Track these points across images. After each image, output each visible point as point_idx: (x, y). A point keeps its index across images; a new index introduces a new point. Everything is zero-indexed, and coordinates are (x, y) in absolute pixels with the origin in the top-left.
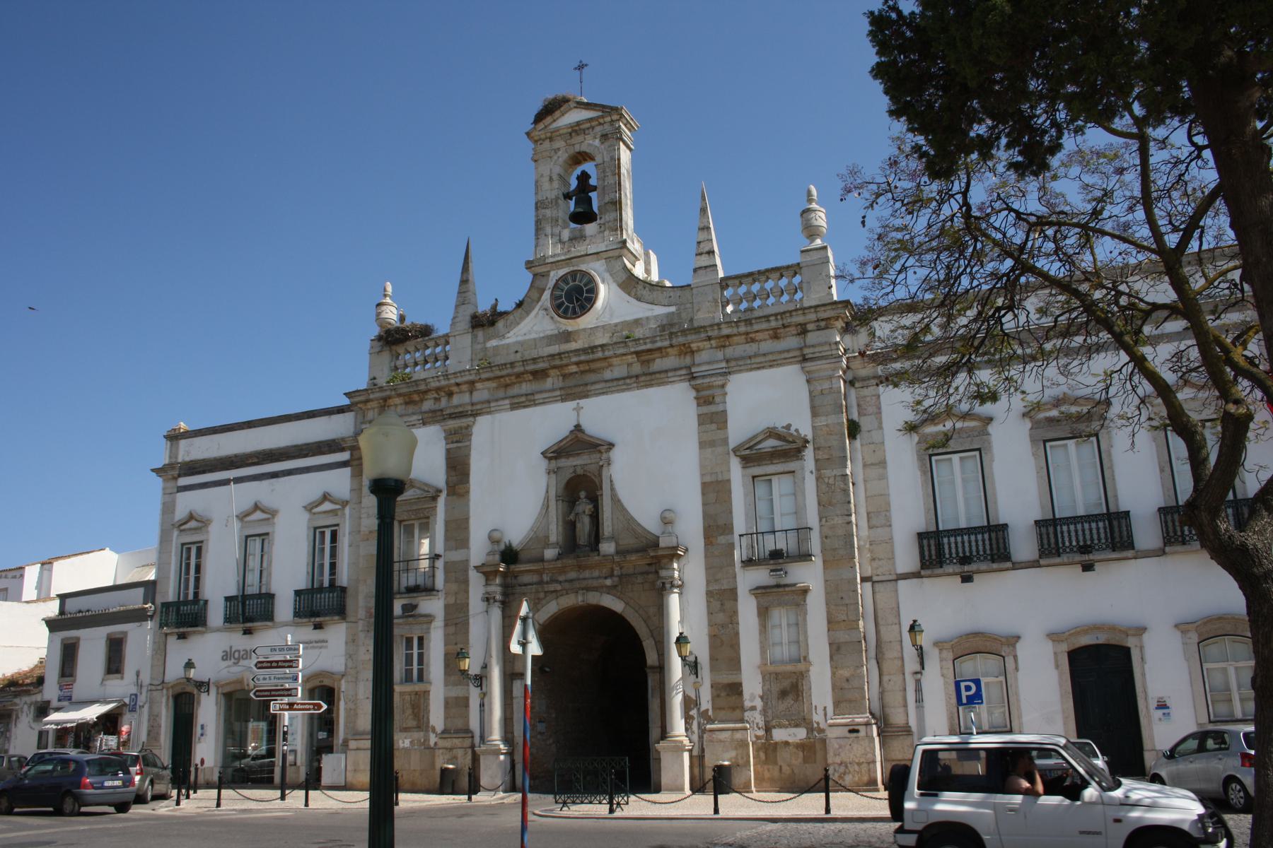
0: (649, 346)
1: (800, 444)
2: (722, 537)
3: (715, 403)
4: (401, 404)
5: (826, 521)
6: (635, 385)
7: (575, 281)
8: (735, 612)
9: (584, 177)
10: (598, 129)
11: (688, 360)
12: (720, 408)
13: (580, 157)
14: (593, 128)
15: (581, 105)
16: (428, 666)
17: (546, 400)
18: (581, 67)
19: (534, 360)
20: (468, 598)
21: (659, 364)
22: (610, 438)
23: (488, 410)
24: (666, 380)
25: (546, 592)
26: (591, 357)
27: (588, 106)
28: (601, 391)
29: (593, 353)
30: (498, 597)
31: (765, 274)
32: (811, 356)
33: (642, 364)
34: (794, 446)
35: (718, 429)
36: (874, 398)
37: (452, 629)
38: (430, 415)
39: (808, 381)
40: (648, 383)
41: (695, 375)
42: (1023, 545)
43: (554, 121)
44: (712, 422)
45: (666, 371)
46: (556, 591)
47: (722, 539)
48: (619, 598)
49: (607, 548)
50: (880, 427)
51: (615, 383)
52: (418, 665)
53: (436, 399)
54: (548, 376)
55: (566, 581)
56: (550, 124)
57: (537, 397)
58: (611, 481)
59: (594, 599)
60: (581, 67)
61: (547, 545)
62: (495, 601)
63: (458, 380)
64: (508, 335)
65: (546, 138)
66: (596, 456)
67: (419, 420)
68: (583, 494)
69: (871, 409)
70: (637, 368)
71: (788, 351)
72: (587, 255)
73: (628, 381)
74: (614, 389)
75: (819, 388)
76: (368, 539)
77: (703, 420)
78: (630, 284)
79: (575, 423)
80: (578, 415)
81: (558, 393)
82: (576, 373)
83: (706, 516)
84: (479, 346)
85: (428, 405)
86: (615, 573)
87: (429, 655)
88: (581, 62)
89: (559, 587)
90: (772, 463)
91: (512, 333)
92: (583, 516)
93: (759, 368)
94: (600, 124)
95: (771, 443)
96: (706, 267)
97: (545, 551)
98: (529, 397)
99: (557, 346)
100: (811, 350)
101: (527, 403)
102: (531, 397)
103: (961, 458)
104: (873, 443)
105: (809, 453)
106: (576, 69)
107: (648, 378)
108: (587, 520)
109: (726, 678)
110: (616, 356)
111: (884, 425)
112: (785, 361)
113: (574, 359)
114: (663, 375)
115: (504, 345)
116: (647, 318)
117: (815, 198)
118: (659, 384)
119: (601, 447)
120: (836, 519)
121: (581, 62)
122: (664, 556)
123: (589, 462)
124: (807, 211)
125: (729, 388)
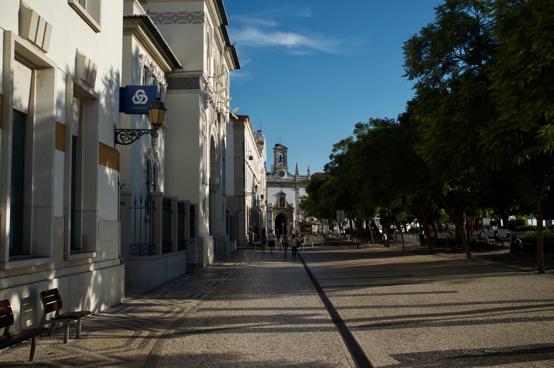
9: (280, 156)
21: (292, 185)
31: (303, 176)
49: (286, 207)
59: (283, 212)
70: (289, 185)
77: (296, 193)
78: (289, 174)
95: (304, 197)
119: (285, 194)
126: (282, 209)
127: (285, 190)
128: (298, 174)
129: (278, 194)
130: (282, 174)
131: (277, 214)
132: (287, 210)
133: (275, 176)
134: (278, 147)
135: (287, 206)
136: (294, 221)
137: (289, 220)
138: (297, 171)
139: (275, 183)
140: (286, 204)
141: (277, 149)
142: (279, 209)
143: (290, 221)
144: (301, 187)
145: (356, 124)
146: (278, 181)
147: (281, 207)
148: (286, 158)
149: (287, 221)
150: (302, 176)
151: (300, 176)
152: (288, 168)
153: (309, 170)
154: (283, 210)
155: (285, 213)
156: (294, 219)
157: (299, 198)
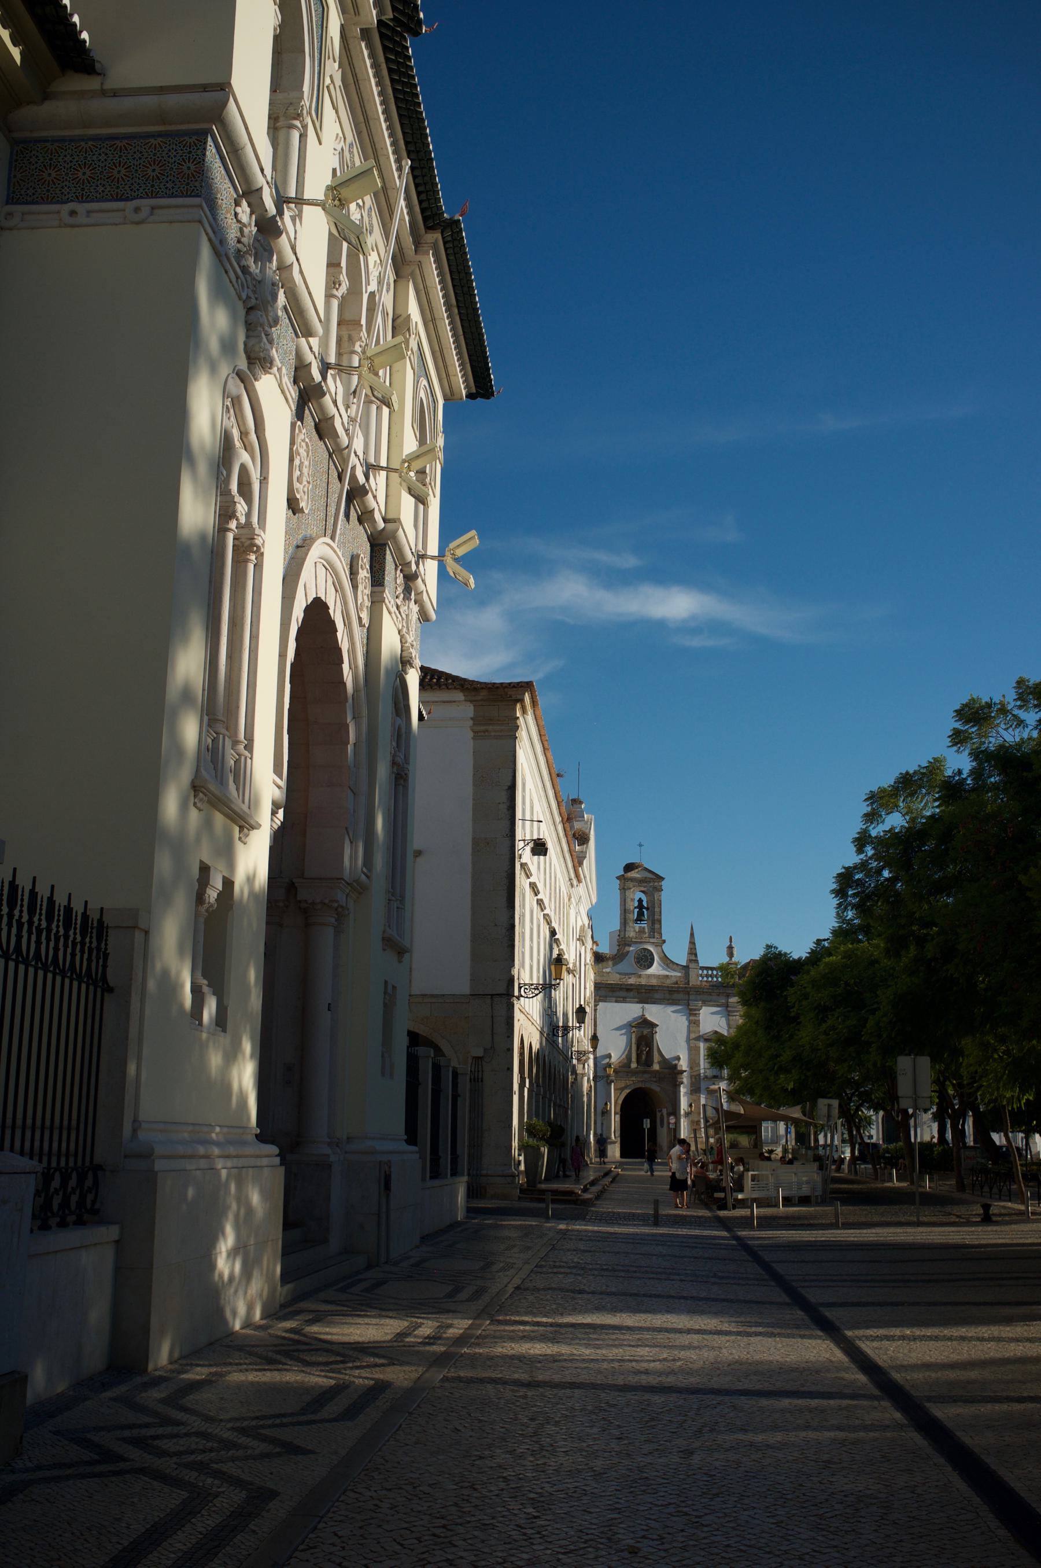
9: (640, 901)
12: (698, 1019)
14: (650, 882)
21: (676, 996)
49: (656, 1067)
59: (648, 1085)
68: (643, 1043)
70: (668, 996)
77: (690, 1022)
78: (667, 961)
109: (696, 1119)
126: (645, 1072)
127: (654, 1012)
128: (696, 961)
129: (630, 1025)
130: (645, 959)
131: (628, 1091)
132: (658, 1076)
133: (622, 967)
134: (633, 874)
135: (659, 1063)
136: (682, 1112)
137: (665, 1111)
138: (693, 952)
139: (621, 989)
140: (656, 1058)
141: (632, 879)
142: (634, 1073)
143: (669, 1114)
144: (705, 1003)
145: (958, 707)
146: (632, 981)
147: (641, 1068)
148: (657, 909)
149: (659, 1115)
150: (707, 968)
151: (703, 968)
152: (664, 941)
153: (730, 948)
154: (646, 1076)
155: (655, 1087)
156: (682, 1107)
157: (698, 1038)
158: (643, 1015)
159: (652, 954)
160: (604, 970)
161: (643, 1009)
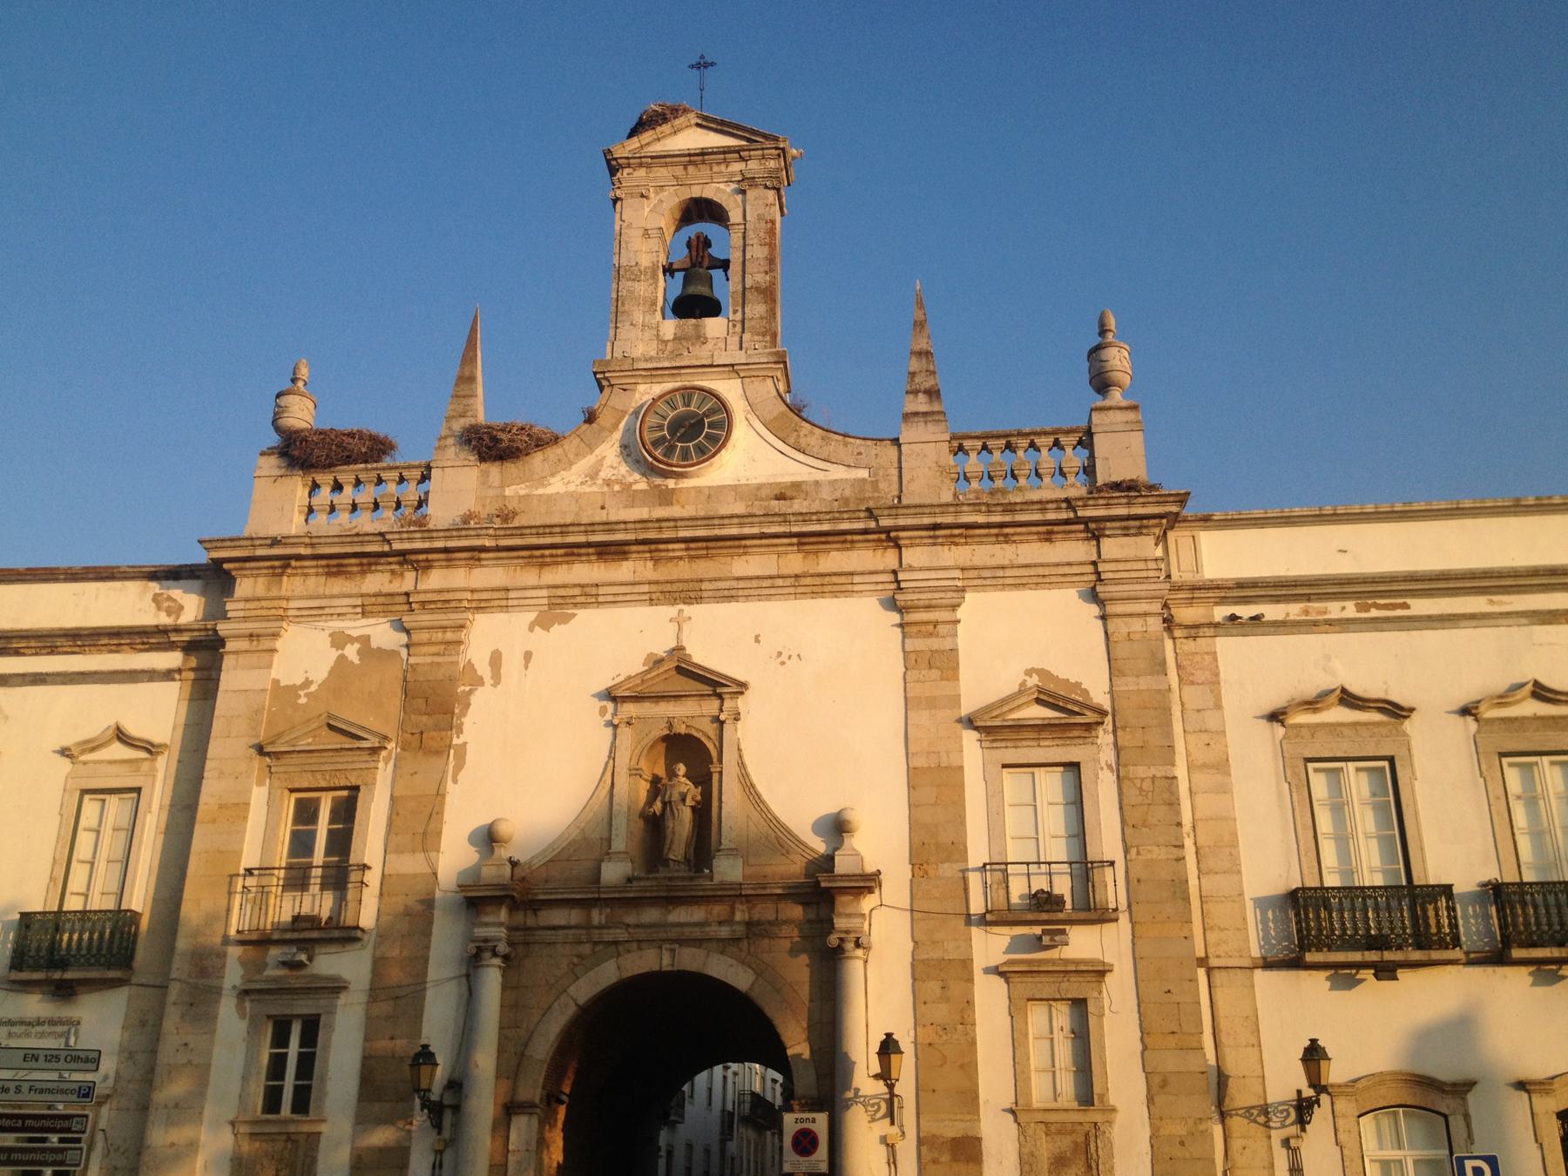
0: (826, 527)
1: (1091, 717)
2: (946, 865)
3: (937, 636)
4: (317, 575)
5: (1138, 853)
6: (792, 590)
7: (689, 406)
8: (970, 1003)
10: (737, 167)
11: (889, 559)
12: (946, 644)
13: (700, 210)
14: (727, 162)
15: (709, 123)
16: (323, 1079)
17: (620, 598)
18: (702, 65)
19: (609, 526)
20: (428, 947)
21: (834, 560)
22: (741, 677)
23: (504, 603)
24: (850, 587)
25: (596, 943)
26: (717, 532)
27: (722, 127)
28: (726, 593)
29: (722, 526)
30: (502, 948)
32: (1111, 575)
33: (804, 557)
34: (1079, 720)
35: (942, 679)
36: (1206, 657)
37: (385, 1007)
38: (381, 600)
39: (1103, 618)
40: (816, 589)
41: (903, 585)
42: (1473, 926)
43: (659, 139)
44: (930, 668)
45: (852, 574)
46: (616, 943)
47: (949, 870)
48: (743, 962)
49: (727, 870)
50: (1218, 706)
51: (755, 583)
52: (297, 1078)
53: (393, 572)
54: (627, 559)
55: (637, 926)
56: (648, 144)
57: (602, 590)
58: (739, 750)
59: (690, 960)
60: (702, 65)
61: (607, 853)
62: (495, 954)
63: (451, 544)
64: (552, 480)
65: (641, 165)
66: (711, 706)
67: (355, 606)
69: (1200, 676)
70: (795, 562)
71: (1069, 564)
72: (711, 366)
73: (780, 582)
74: (752, 592)
75: (1124, 630)
76: (214, 821)
77: (911, 660)
79: (673, 644)
80: (680, 628)
81: (646, 588)
82: (681, 558)
83: (914, 825)
84: (491, 493)
85: (376, 582)
86: (738, 917)
87: (326, 1061)
88: (702, 57)
89: (622, 935)
90: (1039, 746)
91: (558, 478)
92: (681, 807)
93: (1017, 586)
94: (742, 159)
96: (925, 414)
97: (604, 865)
98: (588, 590)
99: (646, 510)
100: (1112, 566)
101: (582, 599)
102: (594, 591)
103: (1358, 770)
104: (1206, 731)
105: (1104, 737)
106: (692, 67)
107: (818, 581)
108: (686, 815)
110: (763, 536)
111: (1224, 703)
112: (1062, 579)
113: (682, 534)
114: (842, 580)
115: (540, 495)
116: (817, 483)
117: (1113, 328)
118: (835, 594)
120: (1155, 849)
121: (702, 57)
122: (844, 890)
123: (698, 712)
124: (1097, 349)
125: (960, 613)
139: (572, 551)
158: (680, 648)
159: (722, 406)
160: (508, 492)
161: (679, 622)
